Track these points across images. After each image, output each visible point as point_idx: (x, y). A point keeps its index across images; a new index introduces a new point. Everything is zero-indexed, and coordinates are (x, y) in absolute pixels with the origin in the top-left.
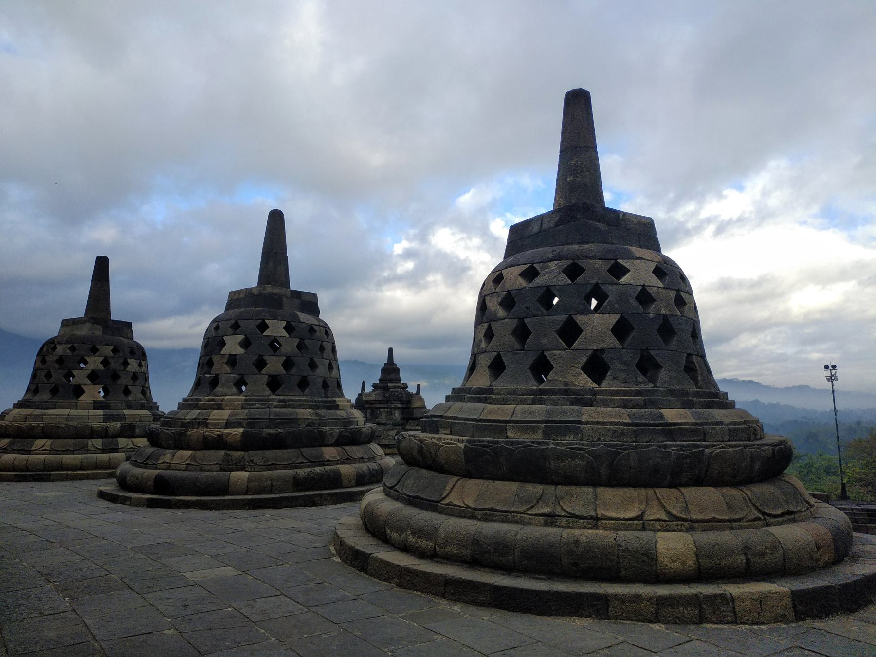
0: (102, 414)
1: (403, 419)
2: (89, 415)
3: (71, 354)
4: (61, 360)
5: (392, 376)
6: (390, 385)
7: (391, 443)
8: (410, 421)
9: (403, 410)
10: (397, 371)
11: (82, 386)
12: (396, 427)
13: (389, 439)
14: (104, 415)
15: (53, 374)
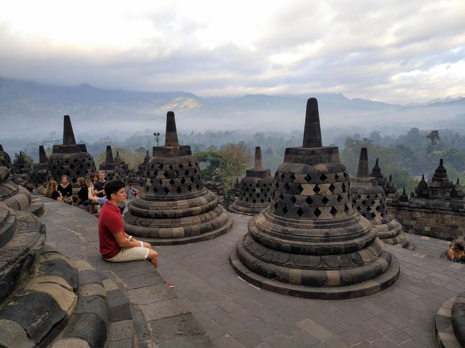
0: (387, 227)
1: (450, 196)
2: (383, 228)
3: (368, 200)
4: (364, 202)
5: (444, 174)
6: (443, 179)
7: (447, 209)
8: (454, 197)
9: (451, 193)
10: (445, 171)
11: (375, 214)
12: (448, 200)
13: (445, 207)
14: (388, 227)
15: (361, 208)
